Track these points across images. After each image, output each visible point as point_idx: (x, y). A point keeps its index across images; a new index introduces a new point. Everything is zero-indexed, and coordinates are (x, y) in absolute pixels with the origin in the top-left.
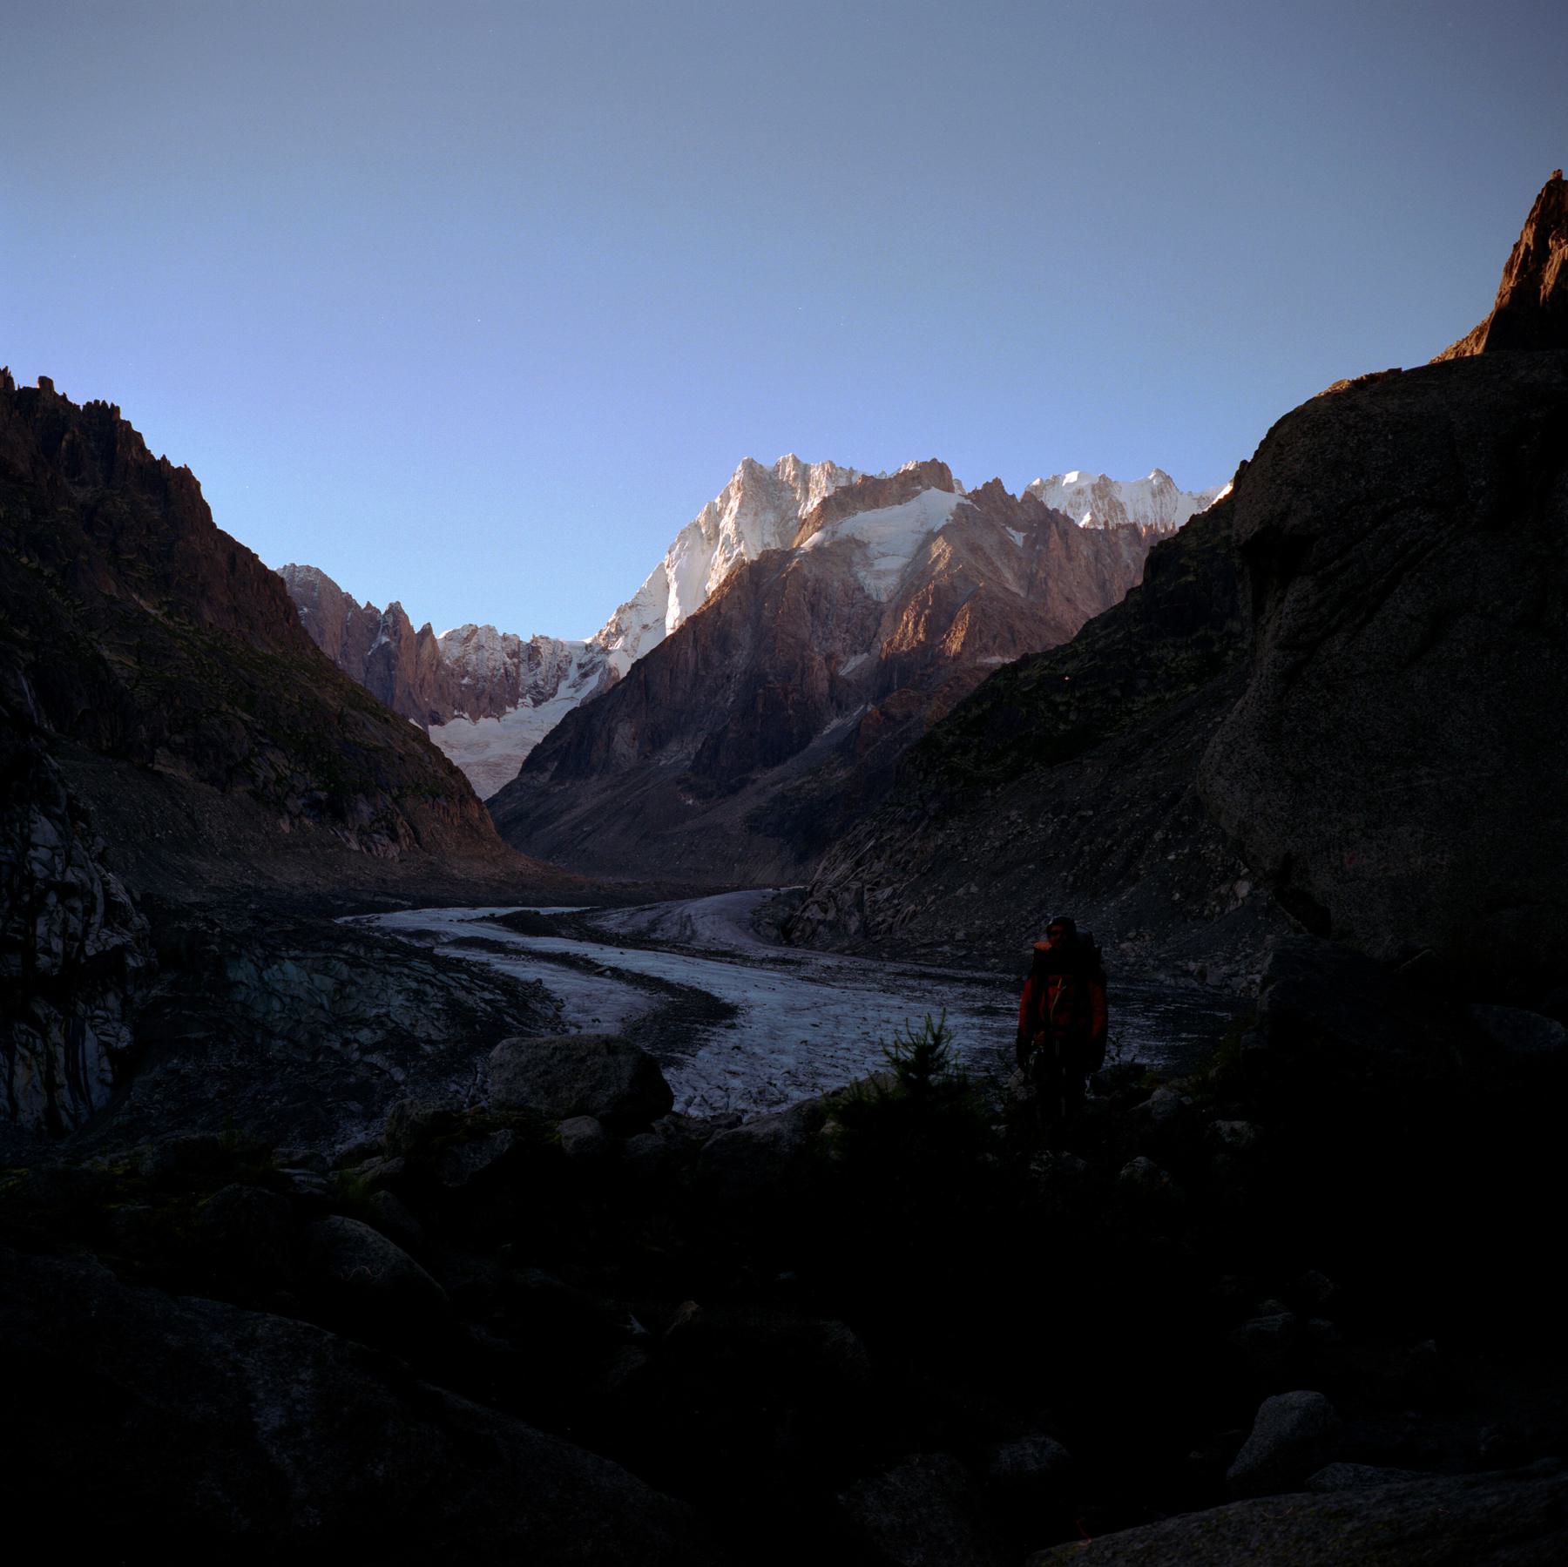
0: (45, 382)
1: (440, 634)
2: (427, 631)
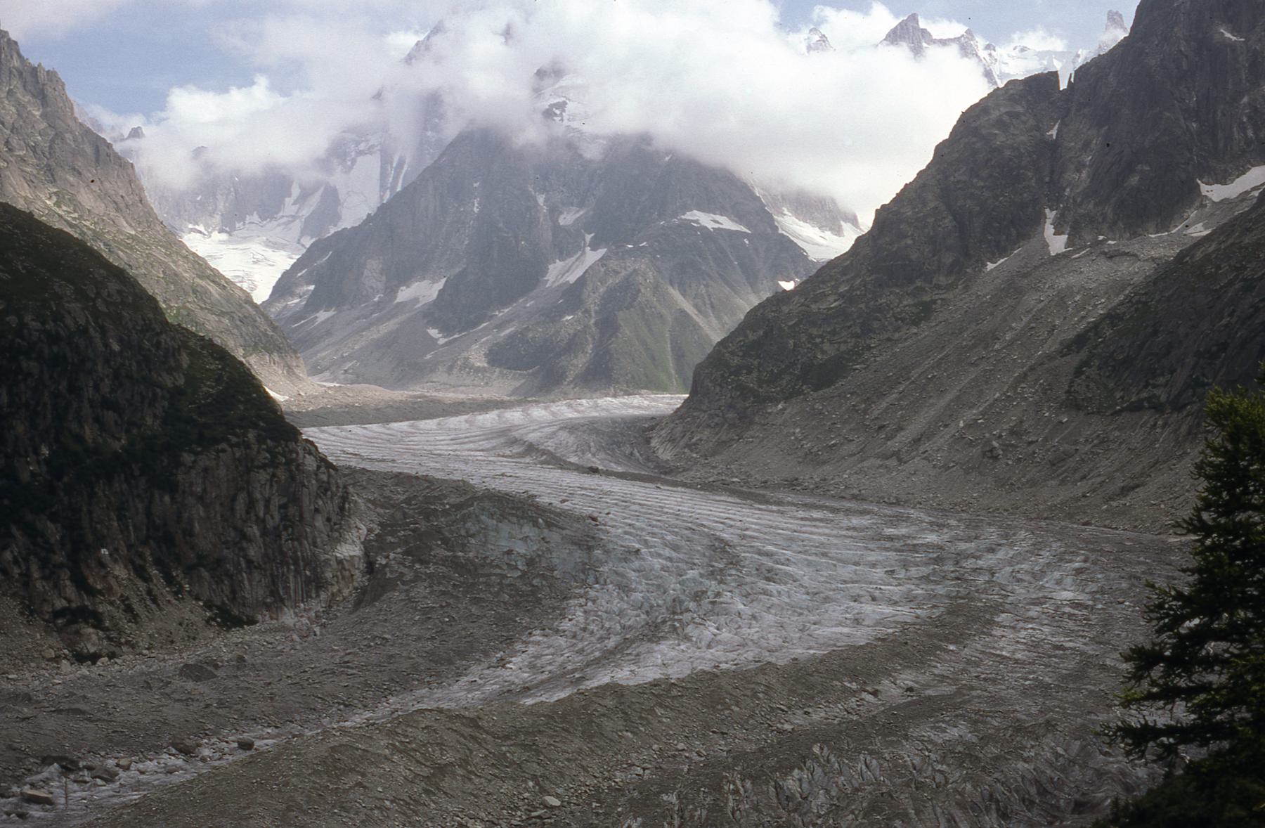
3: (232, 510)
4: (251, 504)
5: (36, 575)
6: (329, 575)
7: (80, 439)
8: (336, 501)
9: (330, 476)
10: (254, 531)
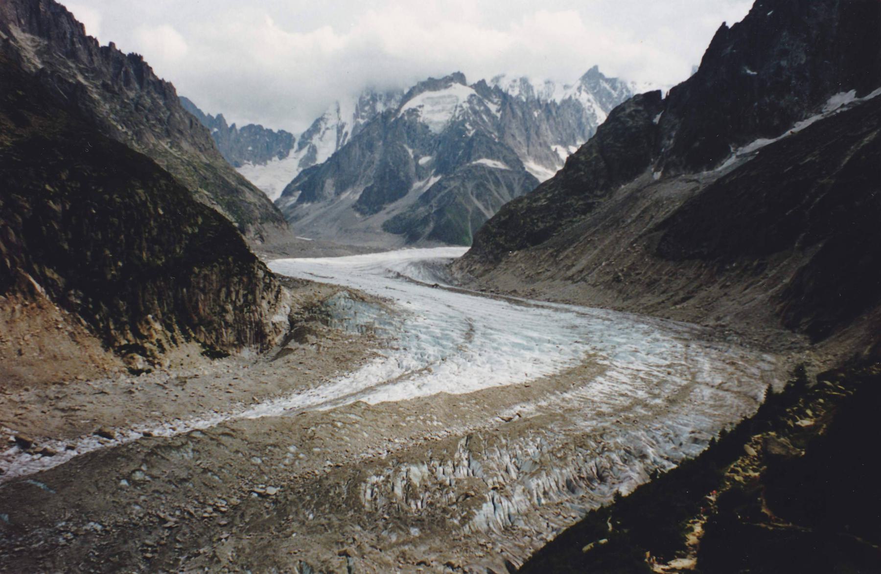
0: (112, 44)
1: (238, 127)
2: (234, 126)
3: (219, 297)
4: (229, 294)
5: (112, 327)
6: (267, 331)
7: (140, 258)
8: (274, 293)
9: (271, 281)
10: (230, 307)
